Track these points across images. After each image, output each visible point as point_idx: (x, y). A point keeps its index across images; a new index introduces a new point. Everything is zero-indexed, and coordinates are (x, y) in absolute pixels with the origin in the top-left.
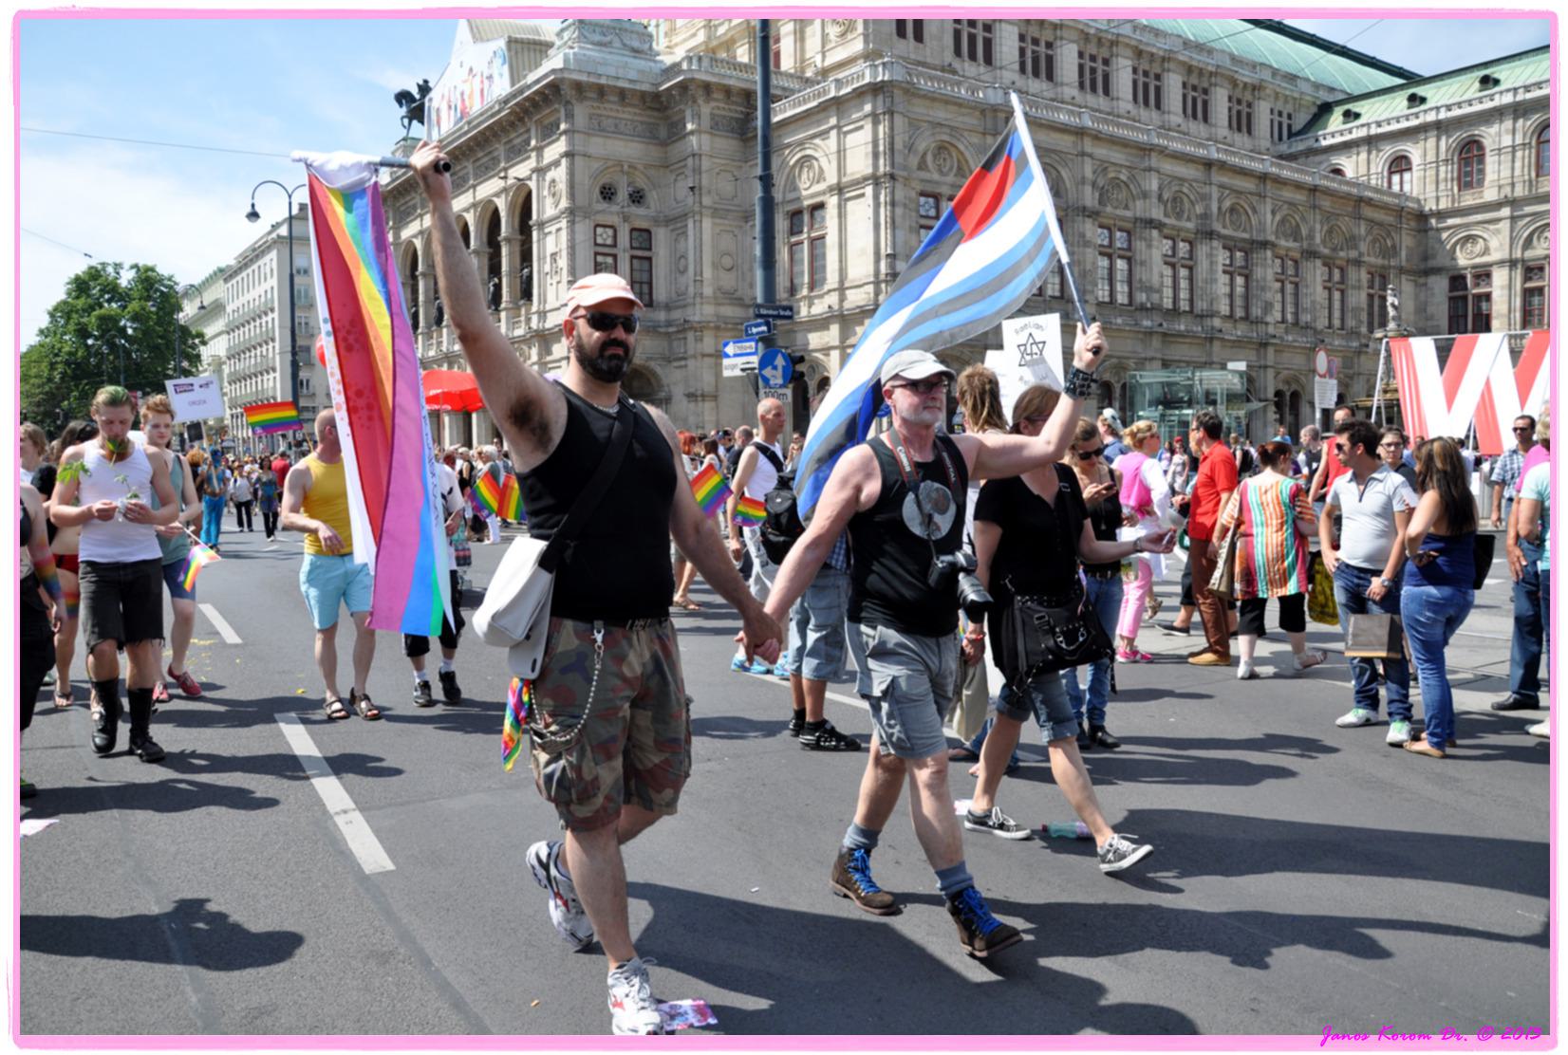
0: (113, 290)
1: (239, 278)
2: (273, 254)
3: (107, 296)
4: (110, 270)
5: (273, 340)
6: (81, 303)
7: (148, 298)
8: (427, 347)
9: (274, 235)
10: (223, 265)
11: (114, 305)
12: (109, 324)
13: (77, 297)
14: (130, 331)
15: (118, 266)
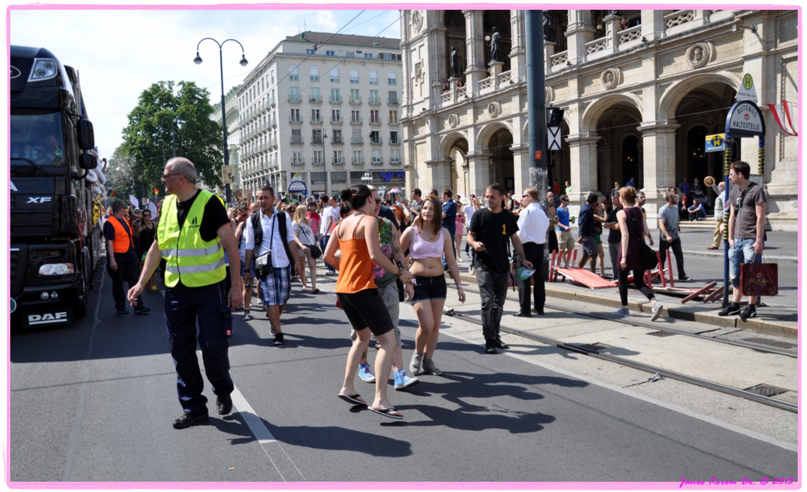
0: (167, 99)
1: (248, 91)
2: (274, 67)
3: (164, 104)
4: (166, 86)
5: (275, 127)
6: (147, 109)
7: (192, 103)
8: (477, 87)
9: (275, 53)
10: (236, 85)
11: (170, 109)
12: (167, 122)
13: (146, 106)
14: (179, 126)
15: (171, 83)
